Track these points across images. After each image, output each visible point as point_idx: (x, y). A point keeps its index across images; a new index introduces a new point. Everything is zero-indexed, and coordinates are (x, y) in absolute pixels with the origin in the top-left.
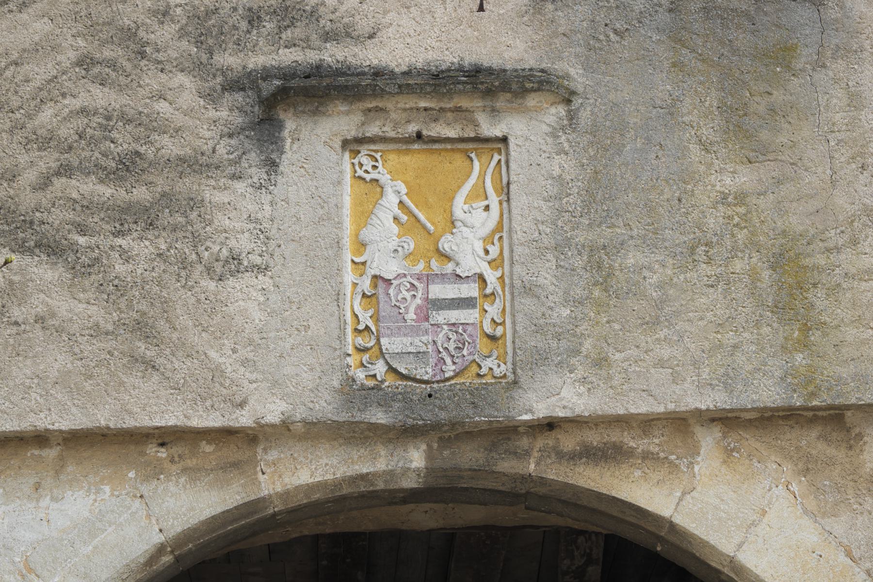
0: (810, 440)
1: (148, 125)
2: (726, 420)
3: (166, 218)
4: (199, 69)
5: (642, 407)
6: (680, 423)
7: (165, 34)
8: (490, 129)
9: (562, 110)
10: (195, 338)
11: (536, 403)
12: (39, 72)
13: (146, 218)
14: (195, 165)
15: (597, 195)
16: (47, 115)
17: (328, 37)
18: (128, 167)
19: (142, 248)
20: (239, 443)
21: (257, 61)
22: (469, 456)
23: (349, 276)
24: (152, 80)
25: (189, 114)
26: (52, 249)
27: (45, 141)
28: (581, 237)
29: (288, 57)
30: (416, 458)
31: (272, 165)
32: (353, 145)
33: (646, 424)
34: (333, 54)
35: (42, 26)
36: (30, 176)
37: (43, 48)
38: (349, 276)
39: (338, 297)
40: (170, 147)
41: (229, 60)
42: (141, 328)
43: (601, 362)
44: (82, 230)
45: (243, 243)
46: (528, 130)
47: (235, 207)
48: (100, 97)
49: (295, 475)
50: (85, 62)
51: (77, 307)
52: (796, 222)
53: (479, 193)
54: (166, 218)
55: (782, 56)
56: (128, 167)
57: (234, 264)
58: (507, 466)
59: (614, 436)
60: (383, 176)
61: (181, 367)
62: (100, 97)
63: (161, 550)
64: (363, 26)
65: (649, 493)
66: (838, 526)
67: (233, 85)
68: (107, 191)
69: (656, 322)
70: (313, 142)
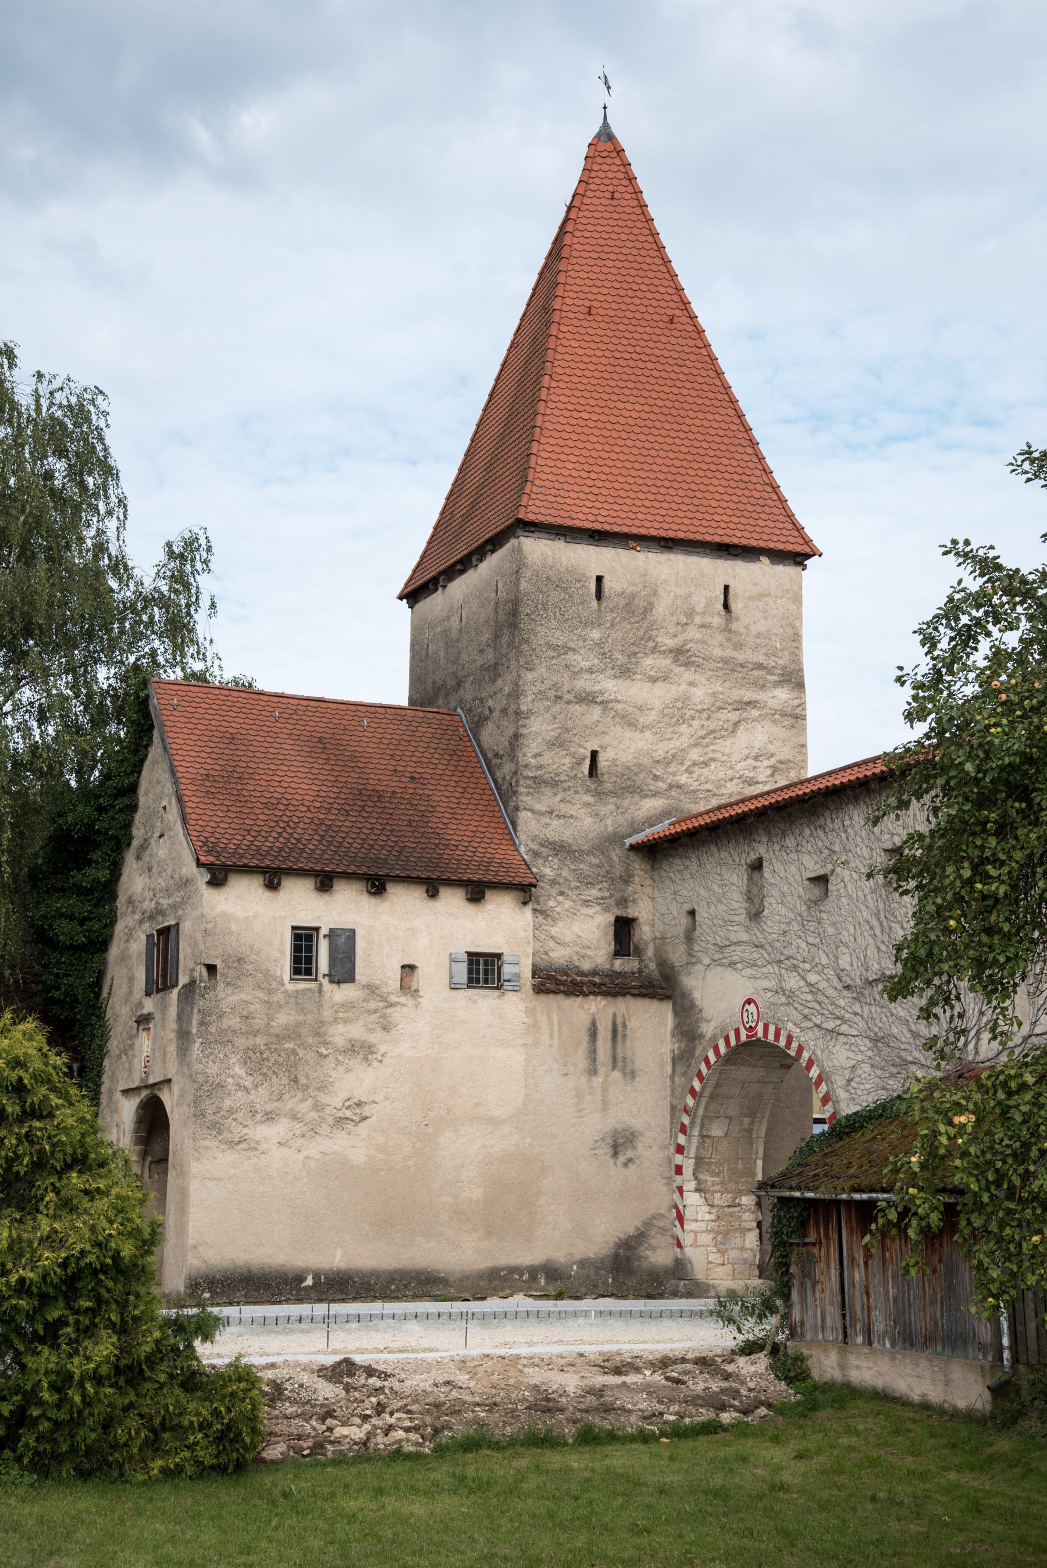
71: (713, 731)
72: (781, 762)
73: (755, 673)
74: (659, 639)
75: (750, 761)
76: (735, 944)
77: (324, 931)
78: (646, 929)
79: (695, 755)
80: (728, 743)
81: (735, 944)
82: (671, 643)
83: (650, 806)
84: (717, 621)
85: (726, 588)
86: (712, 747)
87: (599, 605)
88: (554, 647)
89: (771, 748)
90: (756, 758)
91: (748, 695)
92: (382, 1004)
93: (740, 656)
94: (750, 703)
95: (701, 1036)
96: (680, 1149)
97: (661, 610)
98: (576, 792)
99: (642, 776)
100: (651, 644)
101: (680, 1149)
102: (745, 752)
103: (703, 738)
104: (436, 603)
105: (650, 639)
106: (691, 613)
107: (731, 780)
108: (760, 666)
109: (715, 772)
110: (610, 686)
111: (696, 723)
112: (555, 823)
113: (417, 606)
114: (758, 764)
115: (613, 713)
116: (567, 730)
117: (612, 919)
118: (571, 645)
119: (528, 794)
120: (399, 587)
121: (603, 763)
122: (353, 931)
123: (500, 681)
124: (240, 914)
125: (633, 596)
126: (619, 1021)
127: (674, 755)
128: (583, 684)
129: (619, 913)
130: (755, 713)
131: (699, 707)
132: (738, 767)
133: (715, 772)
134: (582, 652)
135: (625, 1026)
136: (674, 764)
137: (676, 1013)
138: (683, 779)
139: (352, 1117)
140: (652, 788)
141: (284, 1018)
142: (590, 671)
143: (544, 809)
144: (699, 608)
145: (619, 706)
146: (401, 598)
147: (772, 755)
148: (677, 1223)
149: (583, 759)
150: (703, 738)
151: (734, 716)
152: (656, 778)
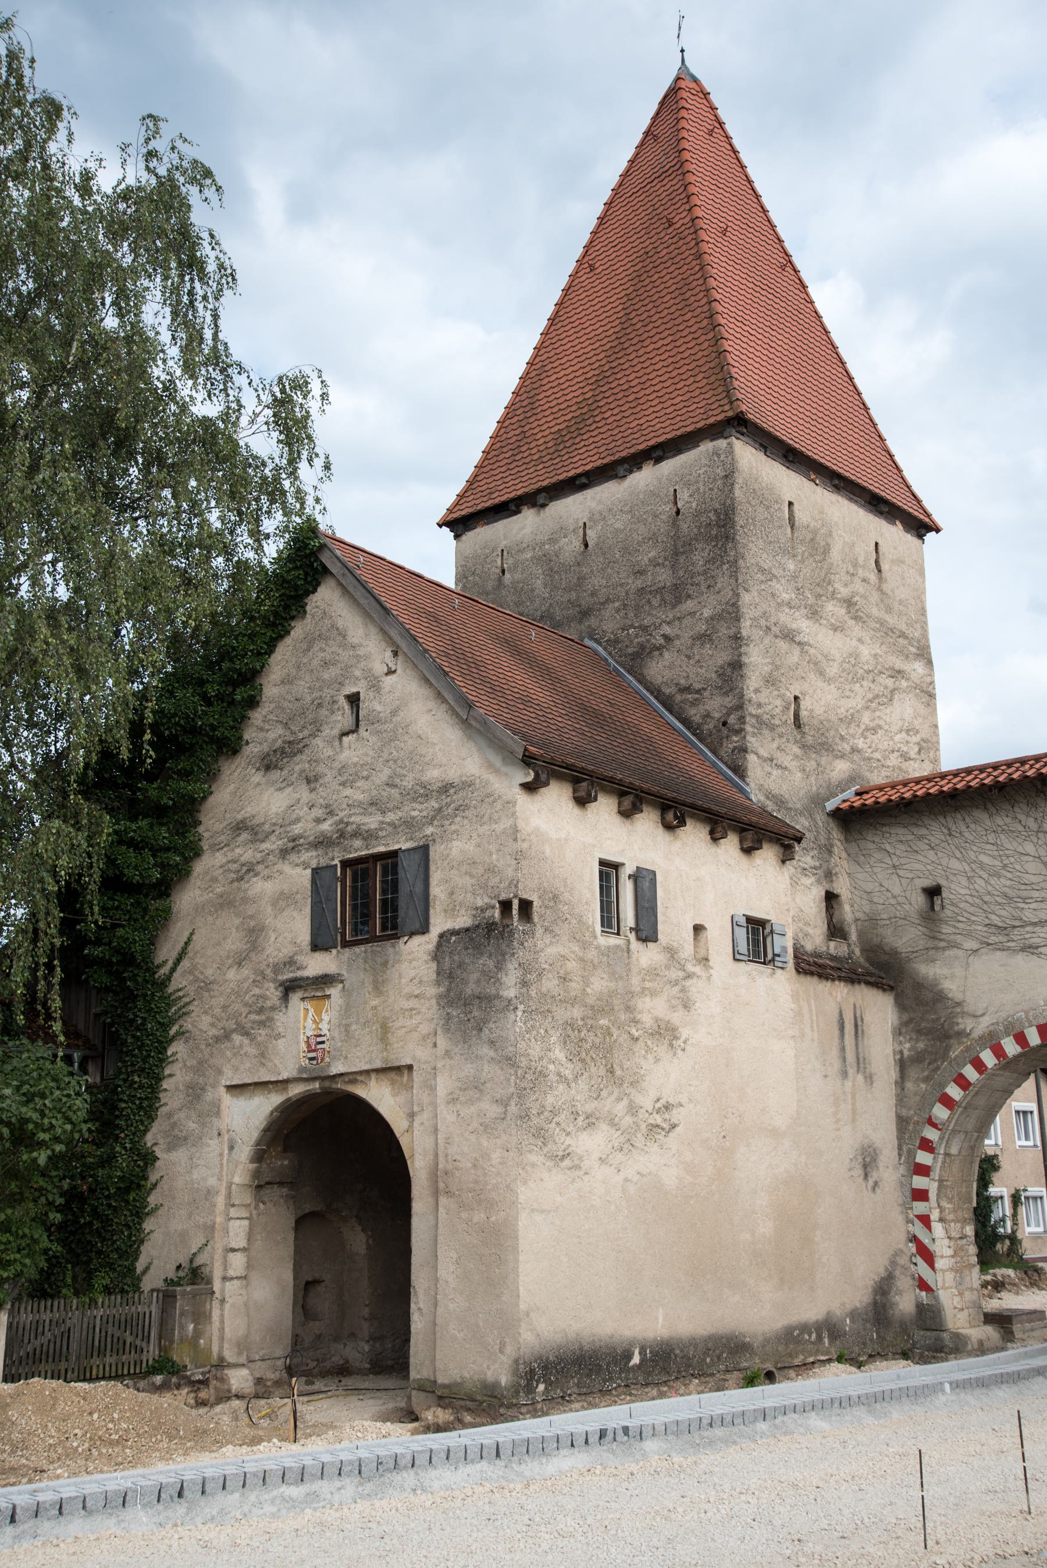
0: (393, 1075)
1: (264, 997)
2: (377, 1071)
3: (268, 1024)
4: (274, 980)
5: (354, 1070)
6: (367, 1072)
7: (268, 972)
8: (328, 993)
9: (341, 985)
10: (272, 1057)
11: (334, 1070)
12: (246, 985)
13: (262, 1024)
14: (273, 1008)
15: (347, 1010)
16: (247, 998)
17: (298, 969)
18: (261, 1010)
19: (263, 1032)
20: (282, 1084)
21: (285, 977)
22: (327, 1084)
23: (302, 1036)
24: (266, 985)
25: (273, 994)
26: (247, 1034)
27: (246, 1005)
28: (344, 1022)
29: (291, 975)
30: (317, 1085)
31: (287, 1007)
32: (303, 999)
33: (361, 1073)
34: (299, 974)
35: (247, 972)
36: (244, 1015)
37: (245, 979)
38: (302, 1036)
39: (298, 1043)
40: (269, 1004)
41: (280, 978)
42: (263, 1055)
43: (346, 1058)
44: (253, 1028)
45: (281, 1030)
46: (334, 991)
47: (282, 1020)
48: (257, 991)
49: (296, 1090)
50: (254, 981)
51: (252, 1051)
52: (387, 1014)
53: (327, 1011)
54: (268, 1024)
55: (385, 964)
56: (261, 1010)
57: (278, 1036)
58: (334, 1086)
59: (355, 1076)
60: (309, 1007)
61: (270, 1064)
62: (257, 991)
63: (272, 1112)
64: (305, 964)
65: (361, 1091)
66: (397, 1099)
67: (280, 985)
68: (257, 1017)
69: (356, 1046)
70: (295, 998)
71: (877, 696)
72: (923, 740)
73: (901, 640)
74: (836, 585)
75: (904, 735)
76: (1035, 924)
77: (629, 869)
78: (847, 908)
79: (866, 719)
80: (888, 711)
81: (1035, 924)
82: (844, 592)
83: (840, 769)
84: (873, 577)
85: (877, 544)
86: (878, 713)
87: (792, 533)
88: (763, 571)
89: (916, 723)
90: (908, 731)
91: (899, 664)
92: (681, 974)
93: (891, 620)
94: (899, 672)
95: (961, 1034)
96: (923, 1170)
97: (835, 554)
98: (788, 741)
99: (832, 733)
100: (831, 589)
101: (923, 1170)
102: (900, 723)
103: (871, 701)
104: (482, 535)
105: (829, 583)
106: (855, 565)
107: (893, 751)
108: (903, 635)
109: (882, 742)
110: (803, 625)
111: (865, 683)
112: (775, 772)
113: (464, 538)
114: (909, 739)
115: (807, 658)
116: (777, 668)
117: (823, 893)
118: (774, 571)
119: (754, 735)
120: (440, 513)
121: (803, 713)
122: (654, 873)
123: (689, 605)
124: (553, 835)
125: (815, 532)
126: (858, 1015)
127: (852, 715)
128: (785, 617)
129: (828, 887)
130: (904, 684)
131: (866, 667)
132: (898, 738)
133: (882, 742)
134: (783, 581)
135: (862, 1020)
136: (853, 725)
137: (901, 1005)
138: (860, 744)
139: (660, 1126)
140: (840, 748)
141: (599, 984)
142: (789, 605)
143: (766, 755)
144: (861, 560)
145: (812, 651)
146: (440, 526)
147: (917, 732)
148: (919, 1260)
149: (790, 704)
150: (871, 701)
151: (890, 683)
152: (842, 738)
